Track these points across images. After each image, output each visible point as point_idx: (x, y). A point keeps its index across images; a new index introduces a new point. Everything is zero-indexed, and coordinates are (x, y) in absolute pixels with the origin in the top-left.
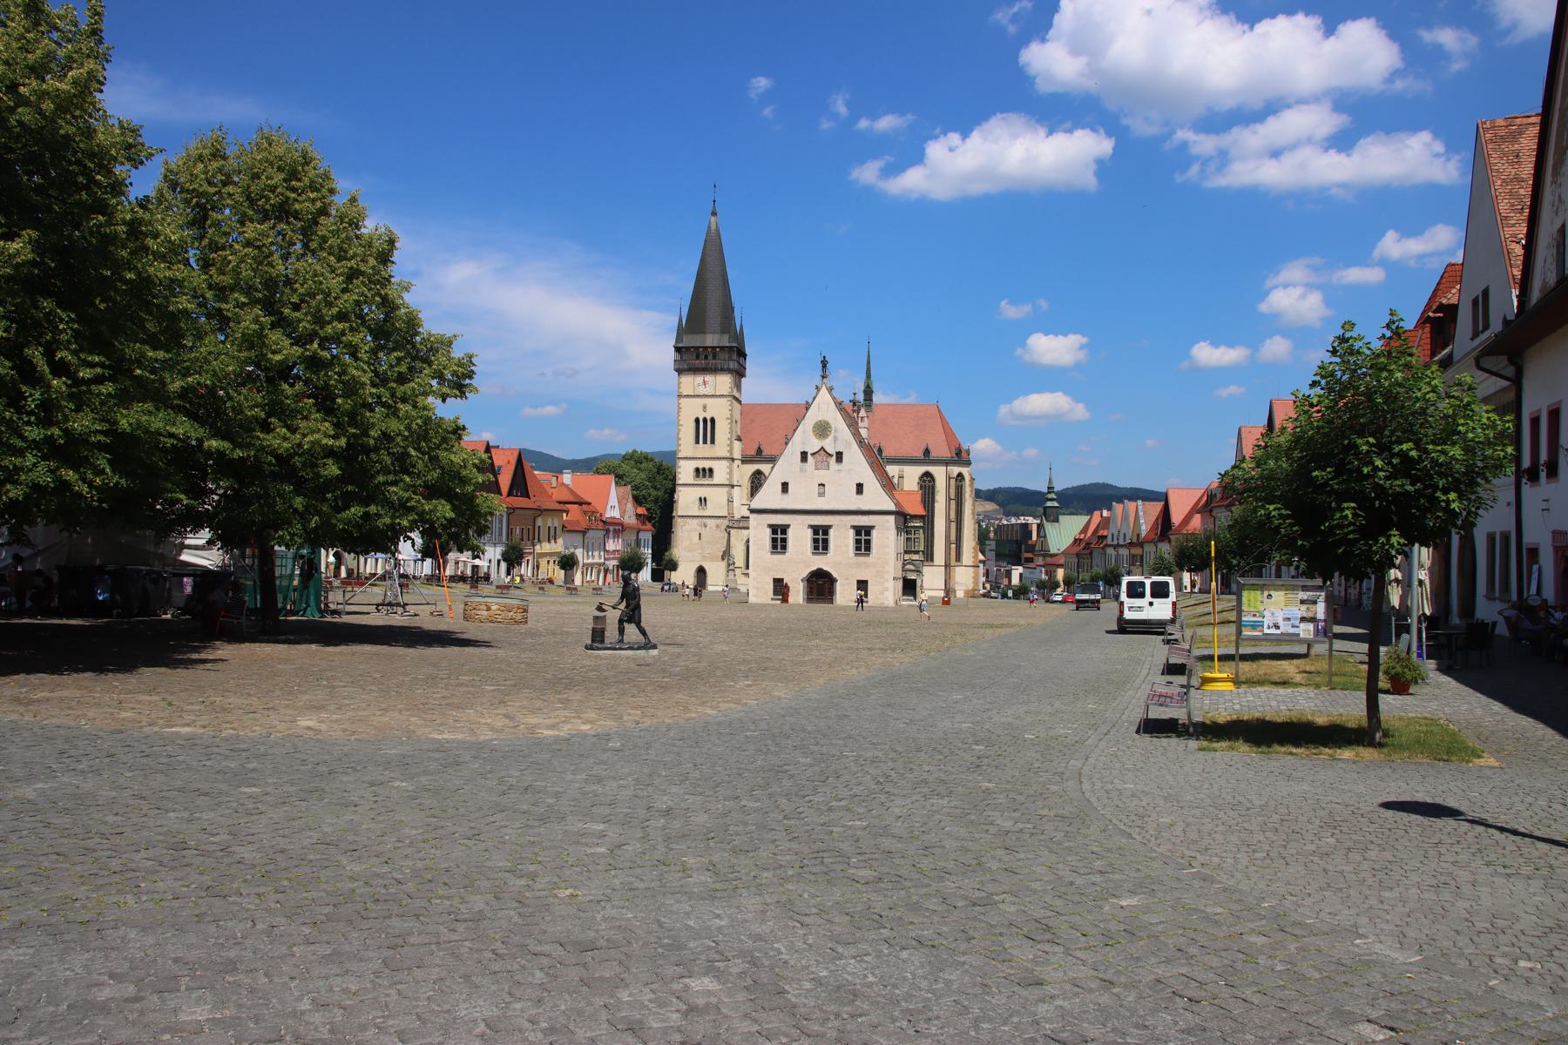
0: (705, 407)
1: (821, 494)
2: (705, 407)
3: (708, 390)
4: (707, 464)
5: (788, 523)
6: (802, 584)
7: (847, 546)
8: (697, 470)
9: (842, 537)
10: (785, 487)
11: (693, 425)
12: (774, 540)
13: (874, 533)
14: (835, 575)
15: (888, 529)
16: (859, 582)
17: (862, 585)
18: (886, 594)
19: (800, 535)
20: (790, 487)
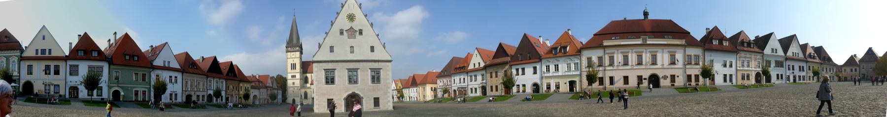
0: (293, 61)
1: (352, 52)
2: (293, 61)
3: (294, 56)
4: (294, 74)
5: (335, 68)
6: (343, 101)
7: (368, 79)
8: (292, 76)
9: (365, 76)
10: (332, 49)
11: (290, 65)
12: (327, 78)
13: (382, 71)
14: (362, 95)
15: (388, 70)
16: (375, 98)
17: (377, 102)
18: (389, 104)
19: (341, 76)
20: (335, 49)
